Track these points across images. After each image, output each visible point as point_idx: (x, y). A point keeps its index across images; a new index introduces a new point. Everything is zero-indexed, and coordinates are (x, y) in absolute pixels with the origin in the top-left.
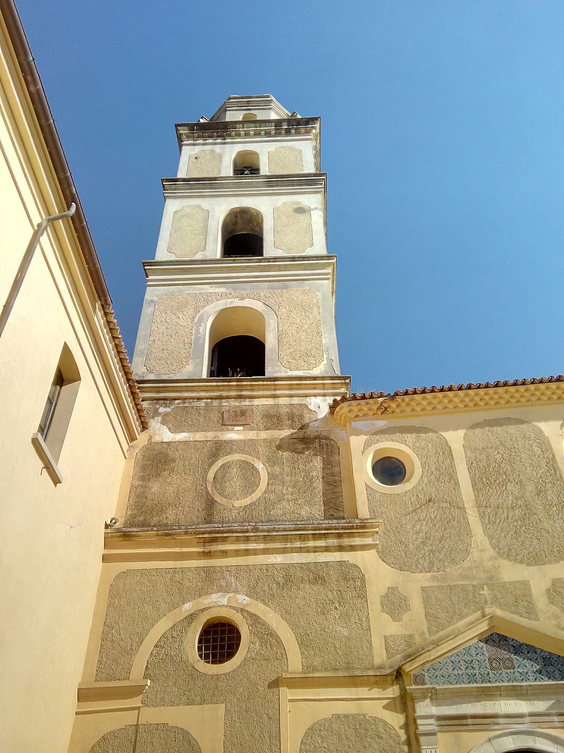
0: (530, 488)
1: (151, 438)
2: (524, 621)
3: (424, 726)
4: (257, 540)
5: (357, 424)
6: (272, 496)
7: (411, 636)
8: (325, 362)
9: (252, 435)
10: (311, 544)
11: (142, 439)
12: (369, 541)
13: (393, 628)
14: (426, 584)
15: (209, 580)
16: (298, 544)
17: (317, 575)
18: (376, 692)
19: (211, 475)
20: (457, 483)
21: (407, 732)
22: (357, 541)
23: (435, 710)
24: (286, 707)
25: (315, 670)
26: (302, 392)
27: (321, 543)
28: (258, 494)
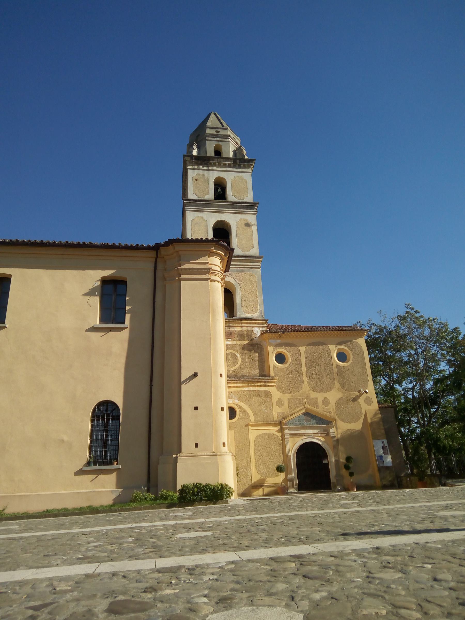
0: (323, 368)
2: (315, 409)
3: (286, 436)
4: (240, 383)
5: (270, 341)
6: (242, 366)
7: (284, 413)
8: (259, 311)
9: (234, 343)
10: (256, 384)
12: (273, 384)
13: (279, 410)
14: (289, 398)
16: (252, 385)
17: (258, 394)
18: (274, 428)
20: (301, 365)
21: (282, 438)
22: (270, 384)
23: (289, 432)
24: (250, 431)
25: (258, 422)
26: (251, 325)
27: (259, 384)
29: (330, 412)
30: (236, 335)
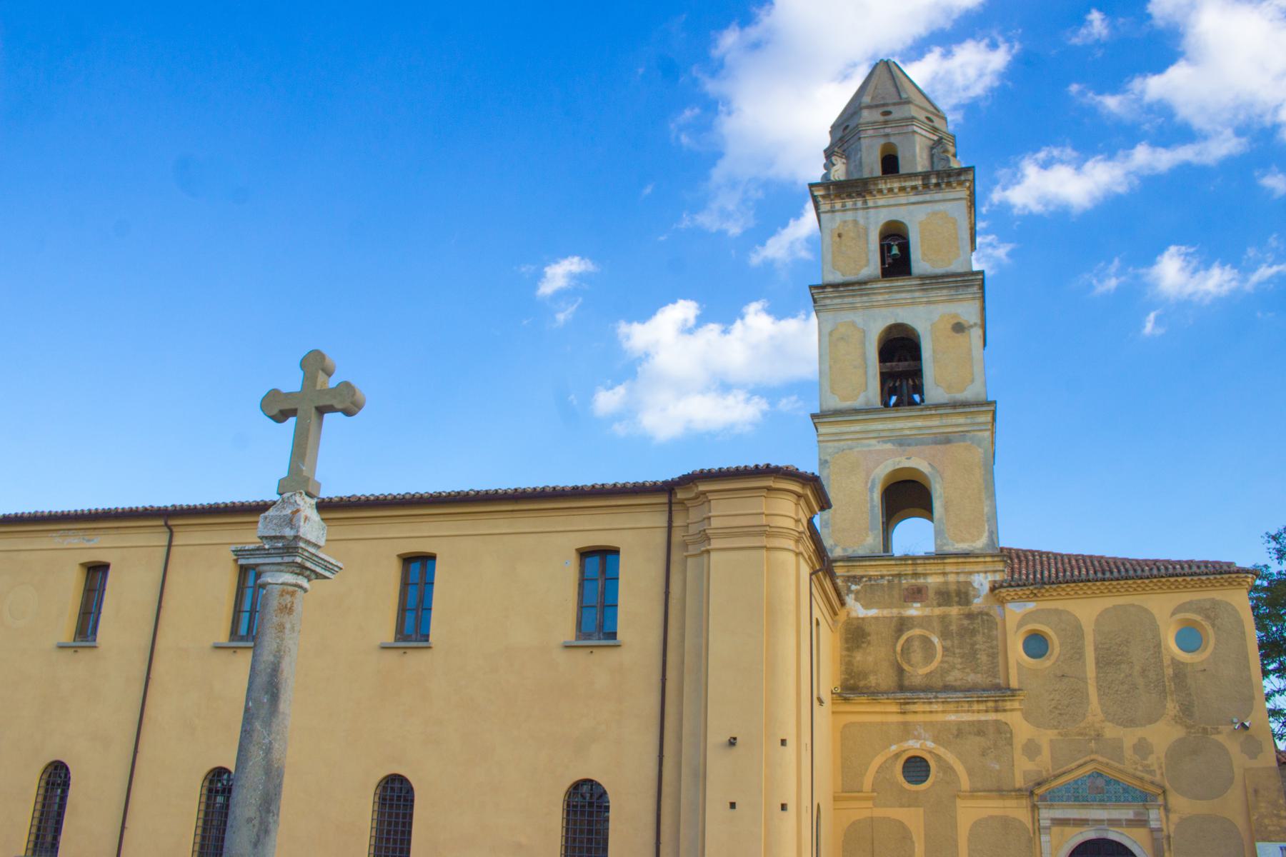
0: (1137, 668)
1: (848, 614)
6: (946, 665)
8: (986, 534)
9: (927, 611)
11: (842, 615)
12: (1016, 705)
15: (906, 731)
17: (979, 729)
19: (898, 648)
28: (934, 665)
29: (1152, 772)
30: (931, 594)
